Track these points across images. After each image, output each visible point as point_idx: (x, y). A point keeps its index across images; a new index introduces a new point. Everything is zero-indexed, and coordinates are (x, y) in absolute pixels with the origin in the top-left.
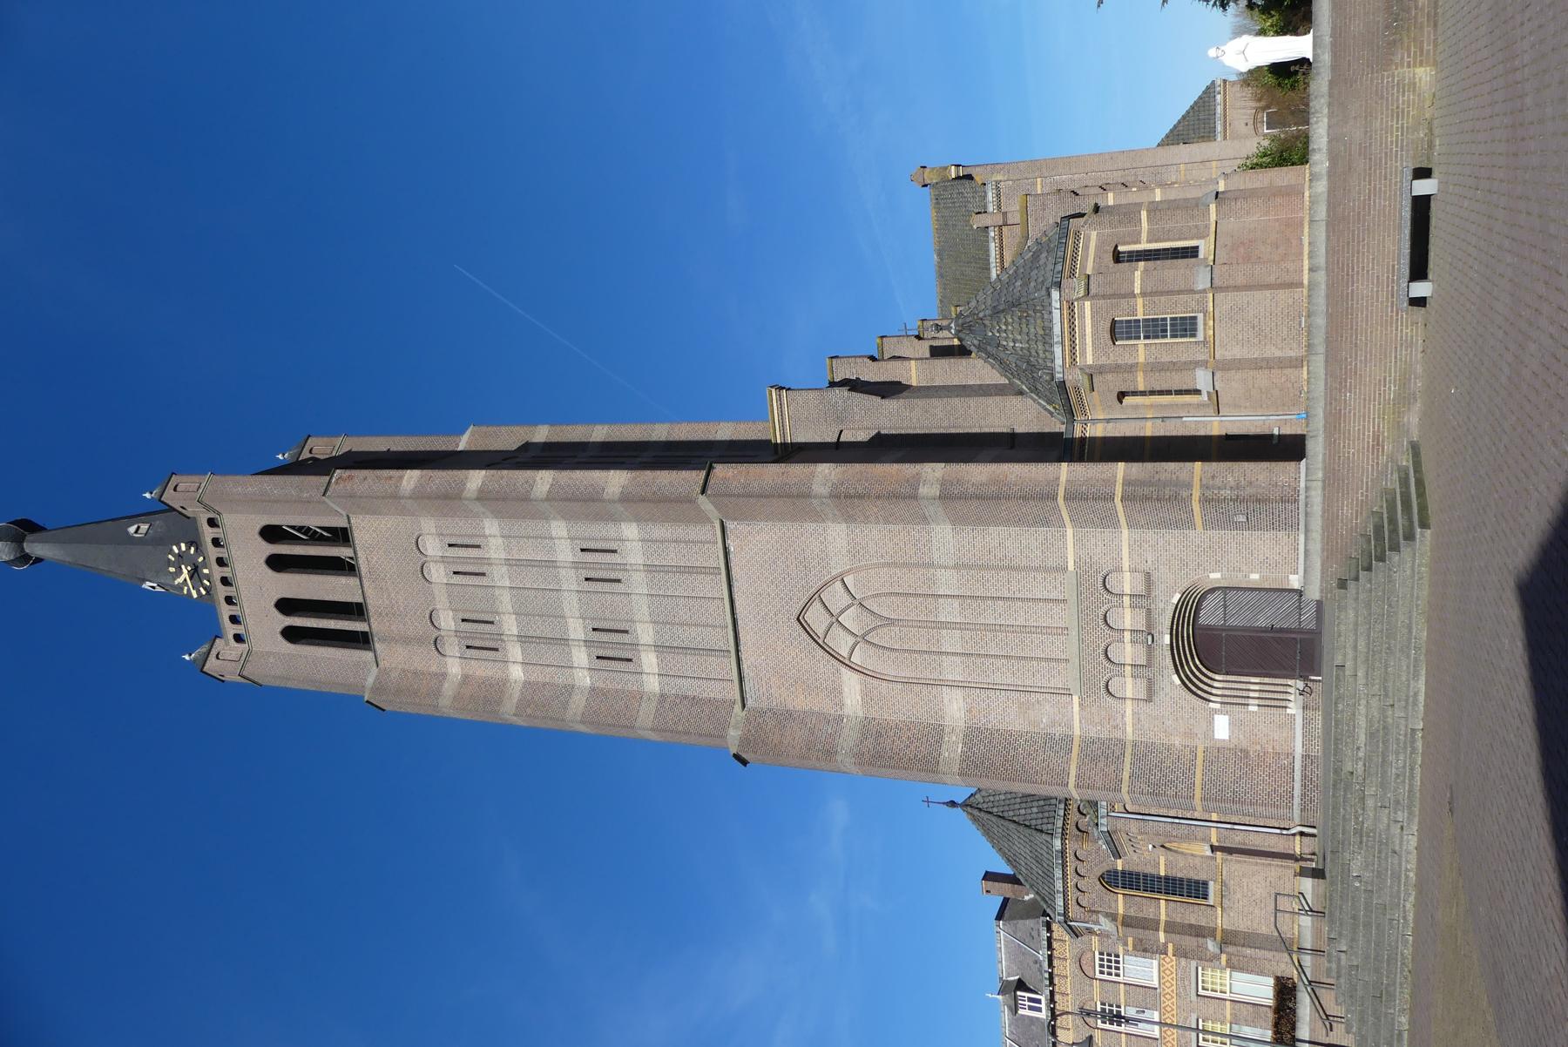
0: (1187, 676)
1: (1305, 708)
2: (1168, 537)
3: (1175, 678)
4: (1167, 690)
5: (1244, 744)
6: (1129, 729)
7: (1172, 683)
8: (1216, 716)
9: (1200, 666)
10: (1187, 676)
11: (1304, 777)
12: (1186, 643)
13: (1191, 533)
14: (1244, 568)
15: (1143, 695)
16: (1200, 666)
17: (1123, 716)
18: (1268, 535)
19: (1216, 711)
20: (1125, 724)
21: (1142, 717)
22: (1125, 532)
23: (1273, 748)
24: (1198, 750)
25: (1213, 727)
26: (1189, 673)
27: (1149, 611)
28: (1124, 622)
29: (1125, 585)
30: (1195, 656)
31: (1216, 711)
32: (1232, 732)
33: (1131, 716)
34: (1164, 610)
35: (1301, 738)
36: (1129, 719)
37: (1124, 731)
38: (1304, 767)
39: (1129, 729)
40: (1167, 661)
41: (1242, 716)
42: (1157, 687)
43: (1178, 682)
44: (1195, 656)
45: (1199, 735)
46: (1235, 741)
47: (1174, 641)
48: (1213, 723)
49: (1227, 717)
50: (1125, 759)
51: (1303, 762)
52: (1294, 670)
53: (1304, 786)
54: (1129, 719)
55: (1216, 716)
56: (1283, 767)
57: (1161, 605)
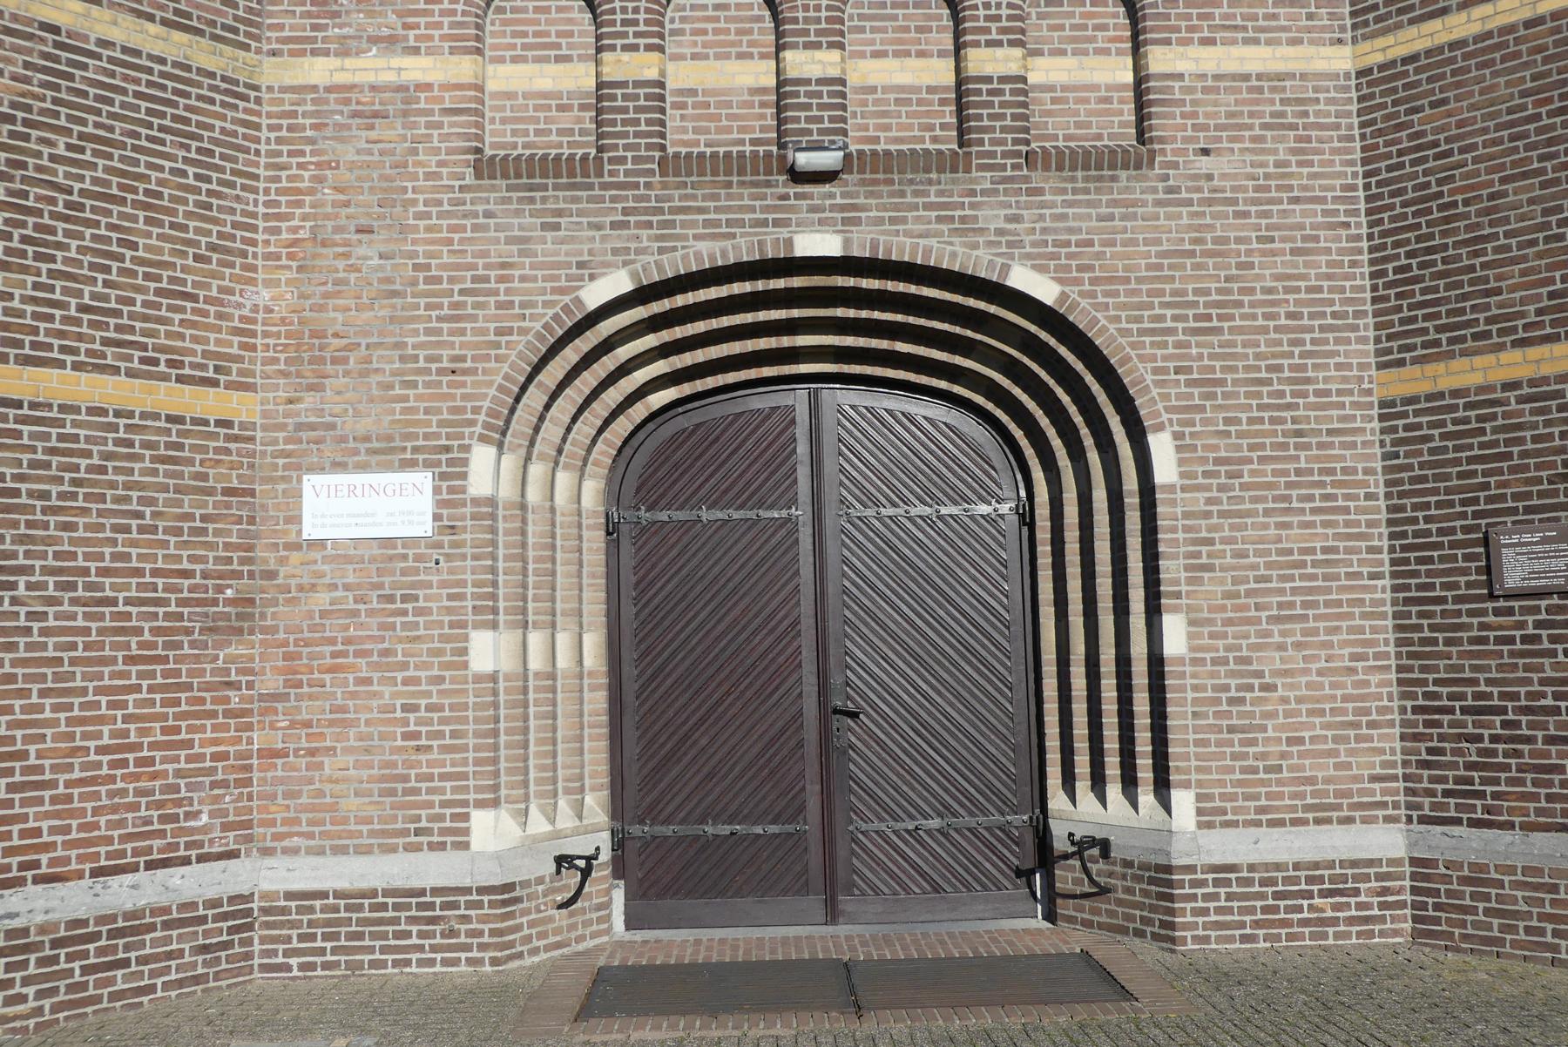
0: (607, 346)
1: (506, 895)
2: (1334, 244)
3: (618, 283)
4: (547, 247)
5: (281, 615)
6: (318, 71)
7: (588, 270)
8: (422, 481)
9: (639, 412)
10: (607, 346)
11: (132, 926)
12: (764, 343)
13: (1360, 348)
14: (1213, 587)
15: (498, 138)
16: (639, 412)
17: (390, 42)
18: (1382, 685)
19: (451, 473)
20: (344, 53)
21: (389, 132)
22: (1341, 60)
23: (271, 754)
24: (236, 395)
25: (363, 467)
26: (624, 352)
27: (952, 164)
28: (877, 55)
29: (1069, 62)
30: (687, 389)
31: (451, 473)
32: (347, 553)
33: (389, 77)
34: (967, 228)
35: (343, 884)
36: (371, 68)
37: (304, 47)
38: (187, 917)
39: (318, 71)
40: (704, 247)
41: (435, 600)
42: (557, 199)
43: (596, 294)
44: (687, 389)
45: (310, 400)
46: (293, 569)
47: (797, 282)
48: (387, 467)
49: (424, 527)
50: (153, 28)
51: (214, 903)
52: (650, 814)
53: (76, 934)
54: (371, 68)
55: (422, 481)
56: (172, 810)
57: (992, 217)
